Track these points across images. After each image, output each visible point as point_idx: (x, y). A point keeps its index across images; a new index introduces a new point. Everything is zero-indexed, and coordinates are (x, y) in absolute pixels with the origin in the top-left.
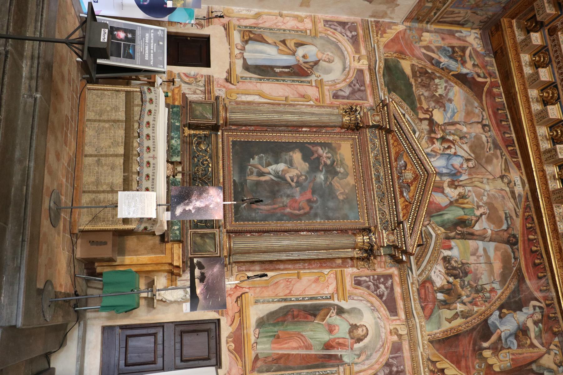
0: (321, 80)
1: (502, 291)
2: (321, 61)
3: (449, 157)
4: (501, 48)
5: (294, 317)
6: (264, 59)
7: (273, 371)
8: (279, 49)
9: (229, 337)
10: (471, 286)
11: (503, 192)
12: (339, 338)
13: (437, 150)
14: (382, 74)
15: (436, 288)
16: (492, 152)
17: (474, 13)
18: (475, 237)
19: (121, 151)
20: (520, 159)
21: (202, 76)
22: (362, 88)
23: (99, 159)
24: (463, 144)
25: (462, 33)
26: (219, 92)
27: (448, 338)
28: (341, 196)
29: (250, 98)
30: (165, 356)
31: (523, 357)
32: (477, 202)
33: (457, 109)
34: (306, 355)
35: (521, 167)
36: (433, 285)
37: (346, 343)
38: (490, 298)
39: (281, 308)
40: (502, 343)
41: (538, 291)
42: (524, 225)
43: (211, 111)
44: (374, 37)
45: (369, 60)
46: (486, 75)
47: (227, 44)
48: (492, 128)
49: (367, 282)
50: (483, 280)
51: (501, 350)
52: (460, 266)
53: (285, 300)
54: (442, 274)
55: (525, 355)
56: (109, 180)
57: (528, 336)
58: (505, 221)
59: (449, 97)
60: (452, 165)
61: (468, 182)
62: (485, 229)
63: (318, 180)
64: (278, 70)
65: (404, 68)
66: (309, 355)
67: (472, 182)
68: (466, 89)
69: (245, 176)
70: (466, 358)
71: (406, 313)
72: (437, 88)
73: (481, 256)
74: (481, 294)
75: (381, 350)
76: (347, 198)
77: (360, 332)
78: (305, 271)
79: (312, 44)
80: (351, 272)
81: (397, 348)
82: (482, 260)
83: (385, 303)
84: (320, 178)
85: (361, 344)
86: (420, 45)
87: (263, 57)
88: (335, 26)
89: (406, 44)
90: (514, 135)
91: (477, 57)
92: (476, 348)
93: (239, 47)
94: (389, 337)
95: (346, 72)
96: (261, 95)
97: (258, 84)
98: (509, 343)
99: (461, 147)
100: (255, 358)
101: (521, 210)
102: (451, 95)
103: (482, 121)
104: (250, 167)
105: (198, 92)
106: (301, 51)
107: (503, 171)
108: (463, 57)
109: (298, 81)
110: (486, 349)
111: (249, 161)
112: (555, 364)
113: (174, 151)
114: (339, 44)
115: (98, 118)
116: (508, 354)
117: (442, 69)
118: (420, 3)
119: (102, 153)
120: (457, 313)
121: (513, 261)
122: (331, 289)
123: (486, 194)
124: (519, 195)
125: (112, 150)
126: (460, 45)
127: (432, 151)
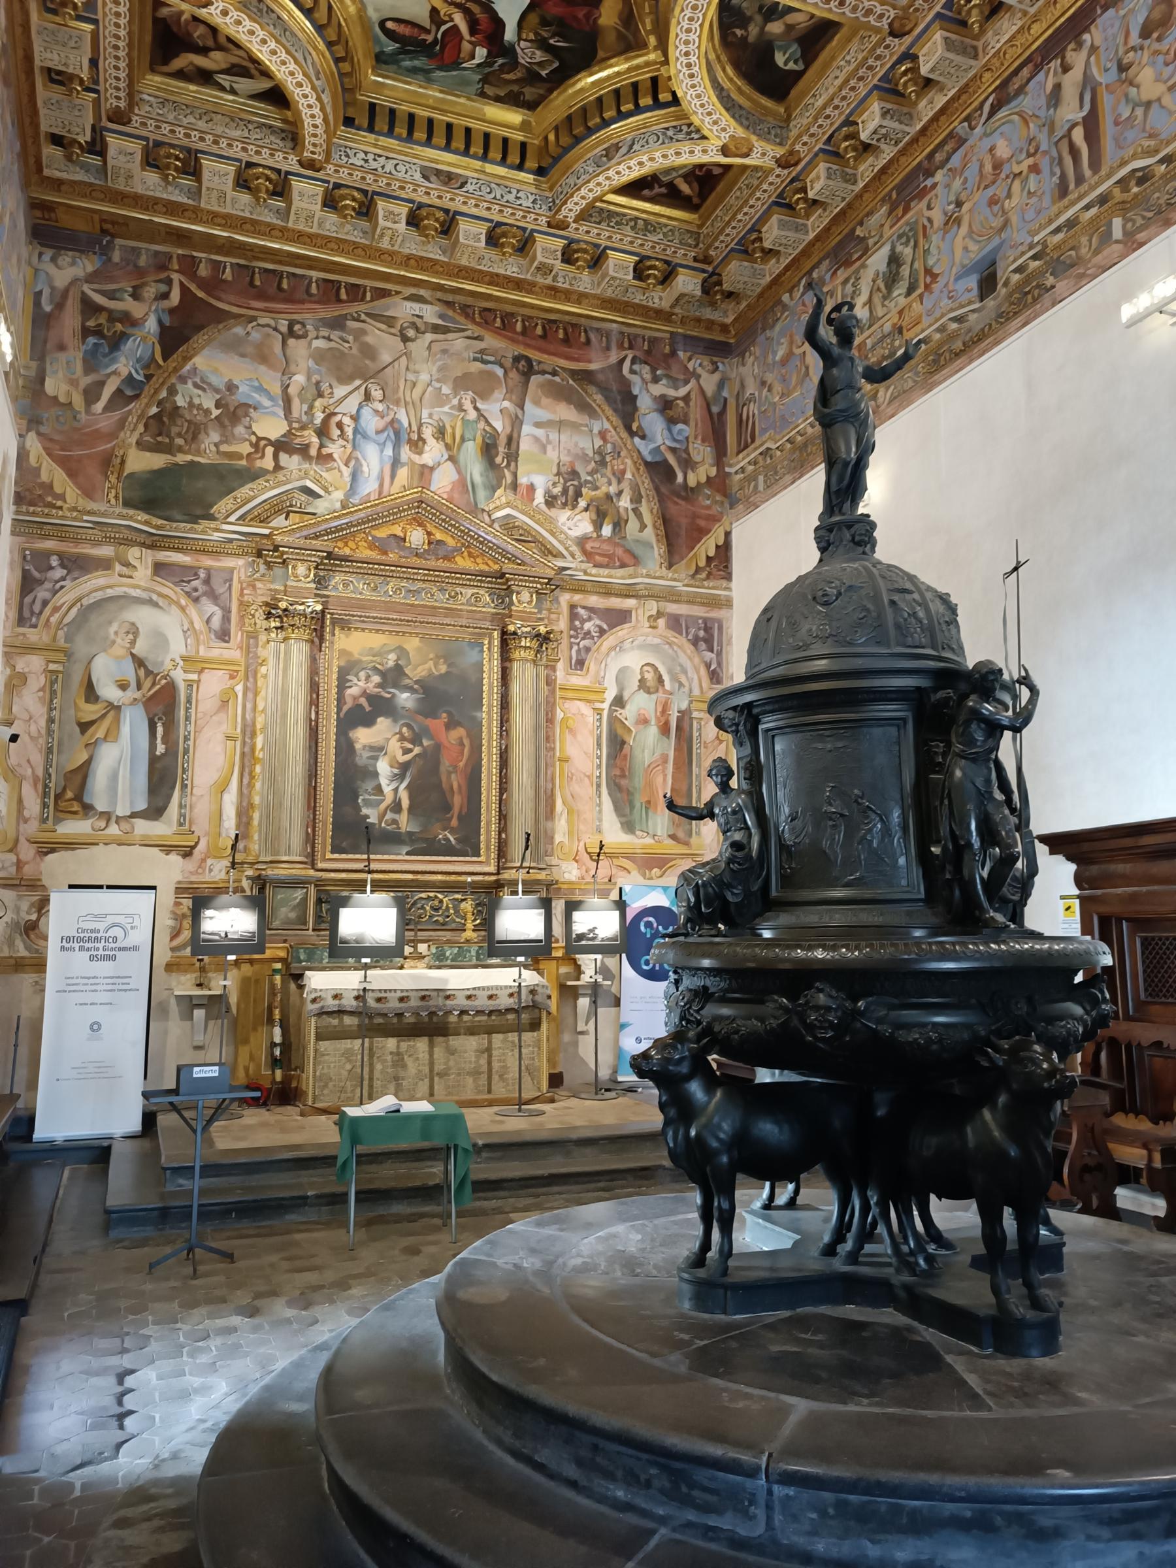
0: (185, 659)
2: (134, 651)
4: (102, 221)
5: (623, 776)
8: (105, 739)
9: (644, 876)
11: (435, 347)
13: (344, 452)
15: (595, 535)
16: (351, 338)
18: (515, 435)
20: (369, 283)
21: (177, 904)
22: (202, 575)
24: (332, 393)
25: (41, 292)
33: (250, 380)
38: (614, 445)
39: (610, 794)
42: (497, 332)
44: (64, 517)
45: (130, 543)
46: (163, 275)
48: (295, 317)
49: (579, 651)
52: (562, 481)
53: (599, 786)
55: (698, 416)
57: (672, 402)
58: (490, 366)
59: (222, 387)
60: (378, 432)
64: (160, 749)
65: (148, 468)
68: (200, 338)
70: (695, 516)
71: (628, 596)
72: (199, 407)
74: (608, 459)
77: (650, 676)
79: (90, 663)
81: (675, 623)
82: (554, 436)
83: (612, 626)
84: (406, 700)
85: (666, 677)
86: (83, 410)
87: (128, 775)
88: (34, 601)
90: (315, 274)
91: (112, 280)
92: (683, 494)
93: (103, 824)
95: (161, 602)
96: (222, 788)
97: (194, 791)
98: (680, 438)
103: (281, 333)
106: (108, 692)
107: (392, 330)
108: (113, 317)
109: (187, 709)
112: (713, 372)
114: (85, 602)
117: (149, 377)
121: (557, 379)
122: (586, 709)
123: (438, 385)
124: (441, 316)
127: (346, 465)
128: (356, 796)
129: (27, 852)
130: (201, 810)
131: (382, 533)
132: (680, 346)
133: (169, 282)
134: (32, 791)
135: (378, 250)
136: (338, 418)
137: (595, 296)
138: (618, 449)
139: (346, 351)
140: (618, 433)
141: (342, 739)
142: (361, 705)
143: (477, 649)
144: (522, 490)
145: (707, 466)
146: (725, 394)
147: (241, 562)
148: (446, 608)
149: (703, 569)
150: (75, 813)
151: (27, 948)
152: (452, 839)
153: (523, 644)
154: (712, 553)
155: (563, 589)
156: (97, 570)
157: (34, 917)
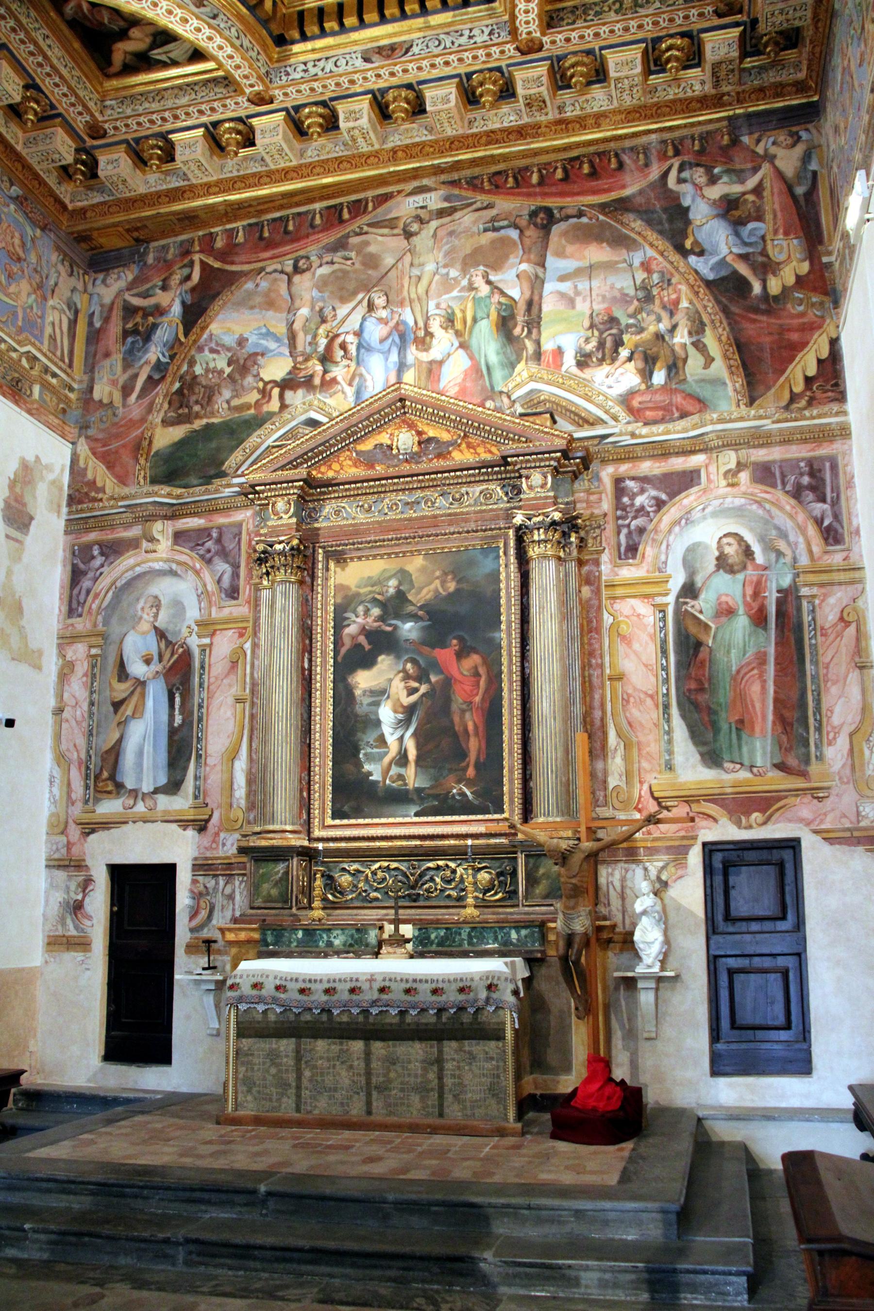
0: (199, 624)
1: (647, 247)
2: (157, 624)
3: (364, 347)
4: (128, 231)
5: (701, 690)
6: (155, 746)
7: (808, 733)
8: (133, 716)
10: (638, 311)
11: (440, 233)
12: (744, 595)
13: (348, 372)
14: (183, 490)
15: (643, 387)
17: (53, 291)
18: (536, 298)
19: (357, 1046)
20: (370, 194)
21: (194, 882)
22: (215, 535)
23: (376, 1087)
24: (335, 315)
25: (93, 313)
26: (229, 845)
27: (744, 365)
28: (449, 585)
29: (240, 779)
30: (775, 952)
31: (781, 211)
32: (462, 290)
33: (259, 328)
34: (777, 663)
35: (386, 194)
36: (636, 392)
37: (755, 579)
38: (662, 273)
39: (683, 717)
40: (753, 253)
41: (646, 171)
42: (510, 193)
43: (271, 865)
46: (186, 261)
47: (125, 828)
48: (301, 253)
50: (625, 284)
51: (767, 256)
52: (596, 333)
53: (666, 707)
54: (613, 371)
55: (777, 207)
56: (416, 1067)
58: (503, 232)
59: (234, 345)
60: (382, 341)
61: (417, 309)
62: (518, 276)
63: (414, 635)
64: (178, 720)
66: (776, 659)
67: (419, 299)
69: (407, 791)
70: (783, 330)
71: (693, 452)
72: (214, 371)
73: (576, 287)
74: (655, 291)
75: (767, 506)
76: (453, 572)
77: (732, 550)
78: (607, 665)
79: (121, 643)
80: (609, 566)
82: (583, 285)
83: (672, 495)
84: (410, 631)
85: (756, 548)
86: (120, 405)
87: (151, 750)
89: (117, 436)
90: (317, 206)
91: (147, 280)
92: (763, 307)
93: (131, 802)
94: (743, 488)
96: (233, 756)
97: (209, 761)
98: (753, 239)
99: (343, 321)
100: (782, 770)
101: (479, 198)
102: (229, 340)
103: (287, 274)
104: (388, 782)
105: (228, 890)
106: (137, 669)
107: (396, 231)
108: (146, 313)
109: (201, 675)
110: (765, 287)
111: (377, 782)
112: (793, 145)
113: (356, 942)
114: (119, 584)
115: (293, 1091)
116: (776, 242)
117: (172, 357)
118: (34, 412)
119: (364, 1082)
120: (693, 344)
121: (584, 220)
122: (644, 609)
123: (443, 271)
124: (447, 199)
125: (356, 1063)
126: (120, 319)
127: (350, 385)
128: (357, 750)
129: (74, 832)
130: (215, 779)
131: (367, 446)
132: (745, 130)
133: (191, 264)
134: (78, 774)
135: (361, 156)
136: (340, 340)
137: (614, 112)
138: (667, 276)
139: (348, 268)
140: (665, 258)
141: (341, 686)
142: (360, 645)
143: (492, 556)
144: (547, 358)
145: (794, 263)
146: (813, 166)
147: (249, 513)
148: (450, 515)
149: (800, 396)
150: (109, 792)
151: (76, 928)
152: (468, 793)
153: (536, 538)
154: (812, 371)
155: (604, 461)
156: (128, 551)
157: (80, 897)
